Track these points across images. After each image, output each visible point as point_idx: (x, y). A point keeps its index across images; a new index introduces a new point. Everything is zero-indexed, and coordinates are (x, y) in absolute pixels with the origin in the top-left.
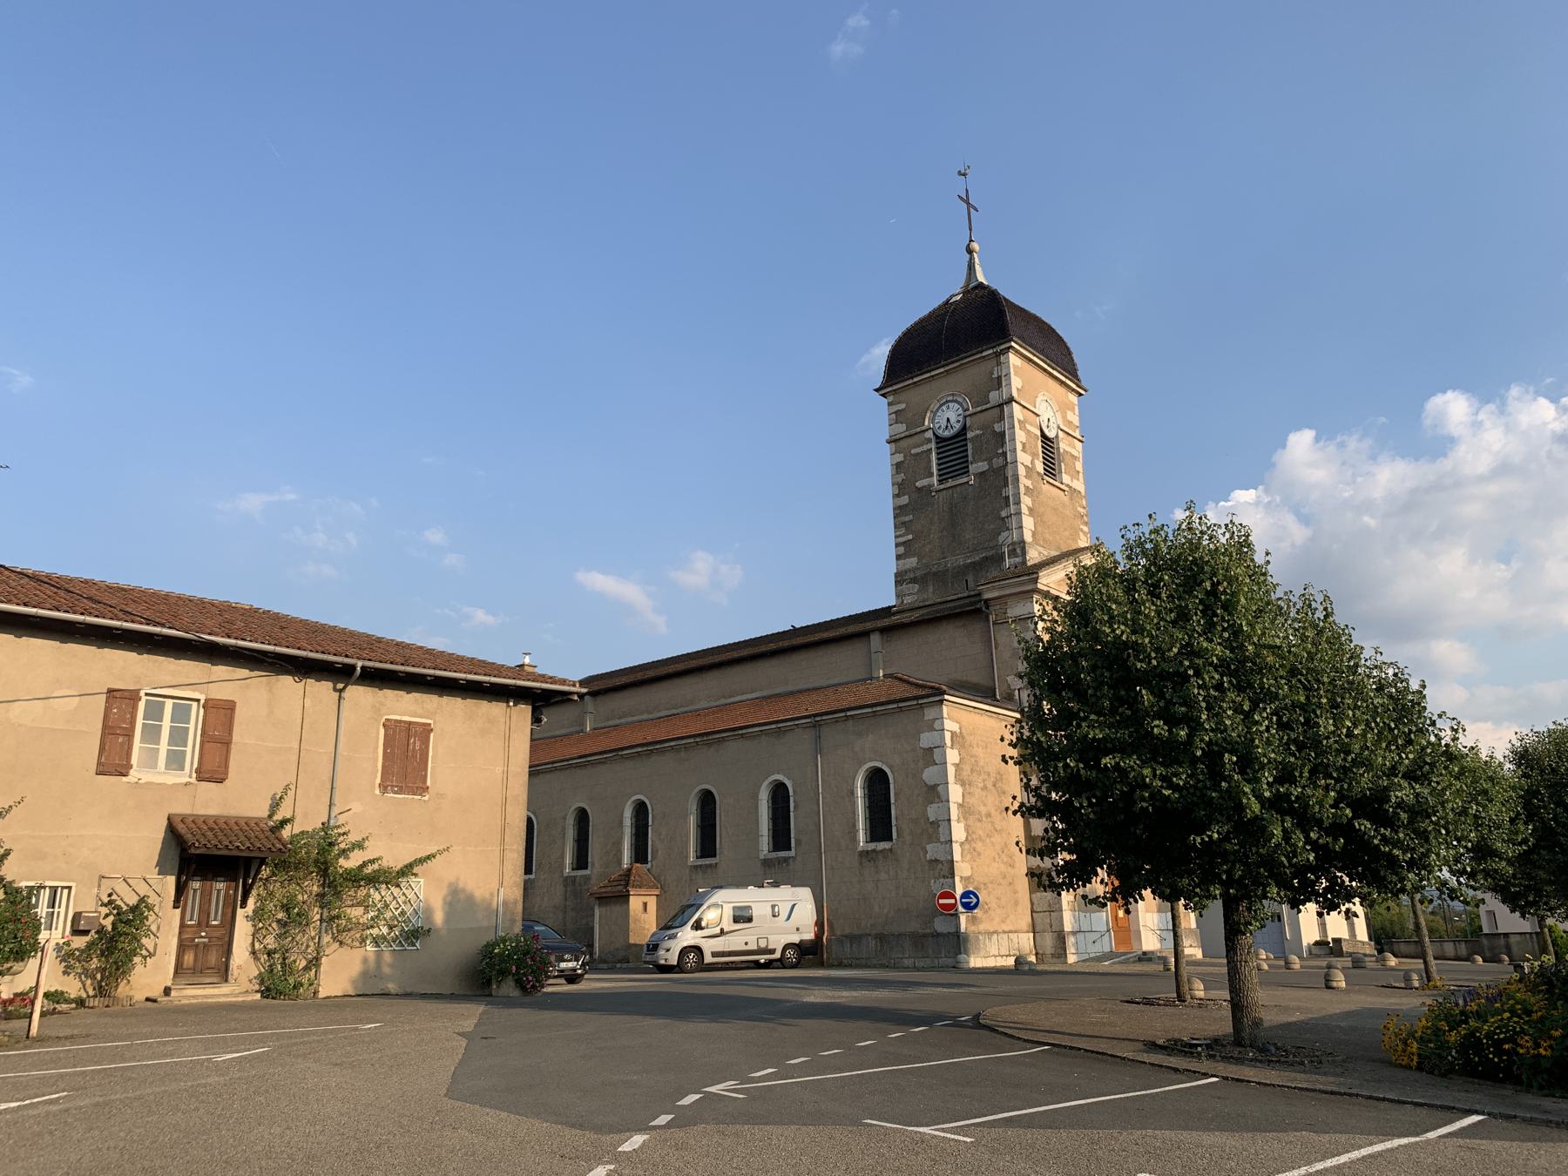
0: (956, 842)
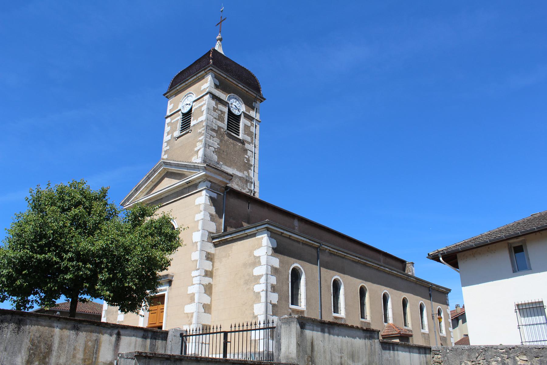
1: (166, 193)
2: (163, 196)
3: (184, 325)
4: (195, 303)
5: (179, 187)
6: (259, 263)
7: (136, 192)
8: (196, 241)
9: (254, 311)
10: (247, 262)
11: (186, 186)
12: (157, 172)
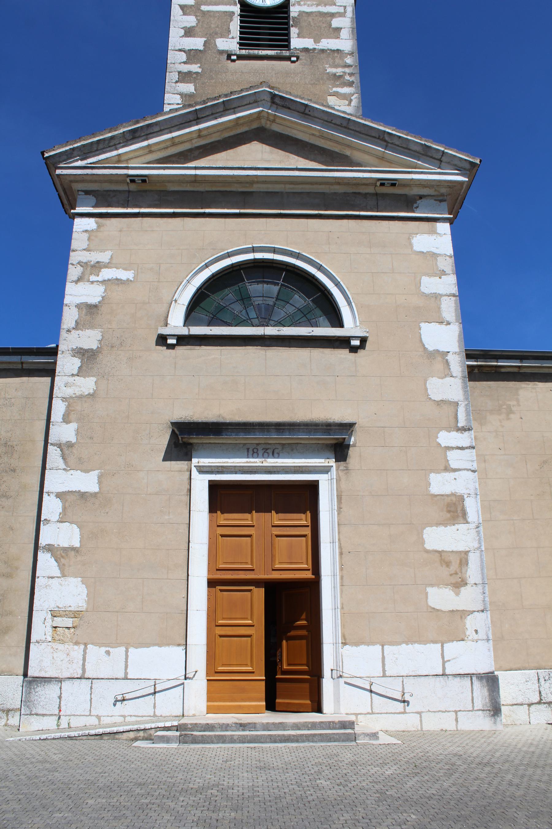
1: (321, 184)
2: (255, 188)
3: (432, 585)
4: (472, 526)
5: (339, 184)
7: (127, 141)
8: (441, 349)
11: (371, 190)
12: (235, 113)
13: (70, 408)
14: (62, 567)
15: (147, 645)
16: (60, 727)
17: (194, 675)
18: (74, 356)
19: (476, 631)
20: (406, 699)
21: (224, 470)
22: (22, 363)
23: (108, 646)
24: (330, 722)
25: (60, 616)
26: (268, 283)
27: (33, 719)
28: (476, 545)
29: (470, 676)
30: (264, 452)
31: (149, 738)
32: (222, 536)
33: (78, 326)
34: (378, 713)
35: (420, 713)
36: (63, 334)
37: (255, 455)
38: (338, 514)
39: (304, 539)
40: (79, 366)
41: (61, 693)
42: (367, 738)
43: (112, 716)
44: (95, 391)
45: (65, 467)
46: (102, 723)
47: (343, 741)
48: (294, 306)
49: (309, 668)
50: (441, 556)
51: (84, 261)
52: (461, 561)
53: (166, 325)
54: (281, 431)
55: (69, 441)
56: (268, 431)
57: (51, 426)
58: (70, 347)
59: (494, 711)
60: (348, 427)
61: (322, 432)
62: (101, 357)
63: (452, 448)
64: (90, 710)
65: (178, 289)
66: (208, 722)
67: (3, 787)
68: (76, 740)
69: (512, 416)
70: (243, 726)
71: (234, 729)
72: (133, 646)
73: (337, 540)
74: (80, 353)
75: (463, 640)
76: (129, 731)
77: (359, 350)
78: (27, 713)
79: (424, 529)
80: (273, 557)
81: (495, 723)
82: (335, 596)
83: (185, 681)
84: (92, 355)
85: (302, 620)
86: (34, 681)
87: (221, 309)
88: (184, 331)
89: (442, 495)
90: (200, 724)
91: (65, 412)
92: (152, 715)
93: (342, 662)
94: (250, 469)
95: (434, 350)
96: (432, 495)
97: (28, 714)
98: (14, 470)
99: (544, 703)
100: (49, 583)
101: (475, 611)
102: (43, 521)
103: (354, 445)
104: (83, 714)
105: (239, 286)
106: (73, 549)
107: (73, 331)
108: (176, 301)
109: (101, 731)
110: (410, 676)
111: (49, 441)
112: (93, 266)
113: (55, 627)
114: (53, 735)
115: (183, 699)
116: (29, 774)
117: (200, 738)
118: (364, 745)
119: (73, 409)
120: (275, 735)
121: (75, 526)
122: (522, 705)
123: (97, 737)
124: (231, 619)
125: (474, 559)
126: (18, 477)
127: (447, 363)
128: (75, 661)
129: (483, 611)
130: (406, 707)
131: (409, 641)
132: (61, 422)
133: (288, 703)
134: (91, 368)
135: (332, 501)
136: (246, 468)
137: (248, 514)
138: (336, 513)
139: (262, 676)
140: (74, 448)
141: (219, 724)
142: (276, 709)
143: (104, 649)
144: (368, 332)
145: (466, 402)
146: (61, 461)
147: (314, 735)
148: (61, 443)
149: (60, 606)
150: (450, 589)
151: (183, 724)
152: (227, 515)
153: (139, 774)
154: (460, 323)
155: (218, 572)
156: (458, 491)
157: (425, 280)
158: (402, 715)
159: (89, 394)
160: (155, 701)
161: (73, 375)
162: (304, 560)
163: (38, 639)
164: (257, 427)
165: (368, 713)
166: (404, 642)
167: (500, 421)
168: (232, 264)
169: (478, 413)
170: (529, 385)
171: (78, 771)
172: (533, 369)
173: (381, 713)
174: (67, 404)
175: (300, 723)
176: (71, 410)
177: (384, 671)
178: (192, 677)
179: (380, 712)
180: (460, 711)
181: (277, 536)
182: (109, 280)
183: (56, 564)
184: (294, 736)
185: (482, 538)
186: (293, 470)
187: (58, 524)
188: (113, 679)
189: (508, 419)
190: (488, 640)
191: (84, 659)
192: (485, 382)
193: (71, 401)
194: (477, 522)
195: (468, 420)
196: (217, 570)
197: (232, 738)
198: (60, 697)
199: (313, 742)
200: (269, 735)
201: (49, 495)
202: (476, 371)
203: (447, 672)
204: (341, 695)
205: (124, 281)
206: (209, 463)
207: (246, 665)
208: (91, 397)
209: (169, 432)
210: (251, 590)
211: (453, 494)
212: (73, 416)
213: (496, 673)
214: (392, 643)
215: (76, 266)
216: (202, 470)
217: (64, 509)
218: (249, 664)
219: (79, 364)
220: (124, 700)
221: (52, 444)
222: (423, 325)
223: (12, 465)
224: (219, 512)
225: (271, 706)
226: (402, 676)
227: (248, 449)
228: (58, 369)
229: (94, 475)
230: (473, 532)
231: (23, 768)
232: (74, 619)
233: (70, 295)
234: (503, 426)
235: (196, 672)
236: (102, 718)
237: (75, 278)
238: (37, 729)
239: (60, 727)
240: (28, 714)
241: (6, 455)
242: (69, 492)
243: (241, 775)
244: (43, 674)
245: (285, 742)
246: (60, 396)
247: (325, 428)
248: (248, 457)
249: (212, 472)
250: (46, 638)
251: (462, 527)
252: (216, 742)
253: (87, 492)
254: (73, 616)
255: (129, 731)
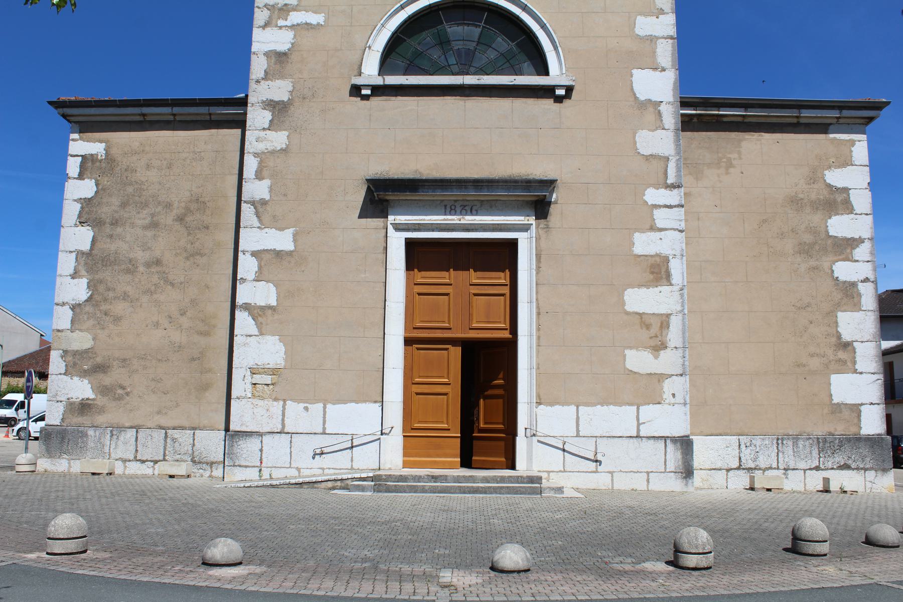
0: (63, 304)
3: (631, 348)
4: (676, 288)
6: (847, 207)
8: (654, 99)
9: (839, 329)
10: (801, 196)
13: (263, 164)
14: (259, 326)
15: (344, 402)
16: (262, 478)
17: (391, 431)
18: (265, 109)
19: (674, 395)
20: (598, 459)
21: (421, 227)
22: (210, 114)
23: (307, 403)
24: (519, 477)
25: (259, 373)
26: (468, 25)
27: (237, 470)
28: (679, 308)
29: (665, 438)
30: (462, 209)
31: (346, 488)
32: (420, 294)
33: (267, 76)
34: (570, 472)
35: (611, 473)
36: (252, 85)
37: (453, 212)
38: (537, 273)
39: (502, 298)
40: (270, 119)
41: (262, 447)
42: (553, 492)
43: (311, 469)
44: (287, 146)
45: (260, 225)
46: (301, 474)
47: (529, 494)
48: (496, 50)
49: (505, 427)
50: (641, 318)
51: (271, 3)
52: (662, 323)
53: (360, 74)
54: (480, 187)
55: (262, 199)
56: (466, 187)
57: (244, 183)
58: (260, 99)
59: (686, 473)
60: (549, 184)
61: (522, 189)
62: (293, 109)
63: (660, 206)
64: (290, 463)
65: (371, 34)
66: (401, 474)
67: (218, 516)
68: (278, 488)
69: (731, 170)
70: (435, 478)
71: (427, 480)
72: (330, 403)
73: (535, 300)
74: (271, 105)
75: (659, 403)
76: (327, 481)
77: (564, 100)
78: (231, 464)
79: (626, 290)
80: (470, 315)
81: (686, 485)
82: (531, 356)
83: (381, 436)
84: (283, 108)
85: (500, 379)
86: (236, 435)
87: (418, 55)
88: (379, 81)
89: (646, 256)
90: (394, 475)
91: (258, 169)
92: (349, 468)
93: (536, 422)
94: (448, 227)
95: (646, 100)
96: (635, 255)
97: (231, 466)
98: (207, 228)
99: (744, 469)
100: (247, 341)
101: (673, 375)
102: (239, 280)
103: (556, 202)
104: (283, 466)
105: (437, 29)
106: (270, 307)
107: (262, 82)
108: (370, 47)
109: (301, 480)
110: (604, 437)
111: (243, 199)
112: (281, 9)
113: (255, 384)
114: (256, 484)
115: (380, 454)
116: (239, 509)
117: (393, 488)
118: (548, 497)
119: (265, 165)
120: (464, 486)
121: (271, 285)
122: (720, 469)
123: (297, 486)
124: (427, 377)
125: (675, 323)
126: (211, 234)
127: (659, 114)
128: (274, 417)
129: (681, 375)
130: (598, 466)
131: (604, 402)
132: (254, 179)
133: (484, 460)
134: (282, 121)
135: (531, 260)
136: (444, 226)
137: (445, 272)
138: (535, 272)
139: (458, 433)
140: (267, 205)
141: (412, 476)
142: (473, 466)
143: (302, 405)
144: (574, 80)
145: (678, 157)
146: (255, 219)
147: (502, 488)
148: (254, 201)
149: (259, 364)
150: (649, 352)
151: (377, 475)
152: (424, 273)
153: (335, 512)
154: (677, 69)
155: (415, 330)
156: (662, 252)
157: (640, 20)
158: (594, 474)
159: (281, 149)
160: (352, 455)
161: (264, 129)
162: (502, 319)
163: (239, 395)
164: (454, 184)
165: (560, 471)
166: (598, 404)
167: (719, 176)
168: (430, 5)
169: (694, 167)
170: (753, 135)
171: (280, 508)
172: (760, 118)
173: (573, 472)
174: (259, 159)
175: (489, 476)
176: (263, 166)
177: (578, 431)
178: (388, 432)
179: (572, 470)
180: (652, 472)
181: (475, 295)
182: (298, 25)
183: (253, 322)
184: (482, 487)
185: (686, 301)
186: (492, 228)
187: (254, 282)
188: (312, 434)
189: (727, 173)
190: (685, 404)
191: (283, 415)
192: (704, 133)
193: (263, 156)
194: (681, 285)
195: (678, 176)
196: (414, 328)
197: (423, 488)
198: (261, 450)
199: (500, 494)
200: (458, 486)
201: (244, 254)
202: (695, 120)
203: (642, 434)
204: (534, 453)
205: (314, 25)
206: (405, 220)
207: (442, 422)
208: (283, 152)
209: (365, 188)
210: (448, 348)
211: (657, 255)
212: (265, 173)
213: (691, 437)
214: (587, 404)
215: (262, 10)
216: (398, 228)
217: (260, 267)
218: (445, 421)
219: (270, 118)
220: (322, 453)
221: (245, 202)
222: (635, 71)
223: (205, 222)
224: (416, 270)
225: (466, 463)
226: (596, 437)
227: (445, 206)
228: (248, 123)
229: (289, 233)
230: (677, 295)
231: (232, 505)
232: (273, 376)
233: (258, 42)
234: (721, 182)
235: (392, 428)
236: (302, 470)
237: (262, 23)
238: (240, 480)
239: (262, 478)
240: (231, 466)
241: (198, 212)
242: (264, 250)
243: (424, 514)
244: (244, 429)
245: (474, 493)
246: (251, 151)
247: (524, 184)
248: (445, 215)
249: (409, 229)
250: (246, 395)
251: (665, 289)
252: (408, 491)
253: (282, 251)
254: (271, 373)
255: (327, 481)
